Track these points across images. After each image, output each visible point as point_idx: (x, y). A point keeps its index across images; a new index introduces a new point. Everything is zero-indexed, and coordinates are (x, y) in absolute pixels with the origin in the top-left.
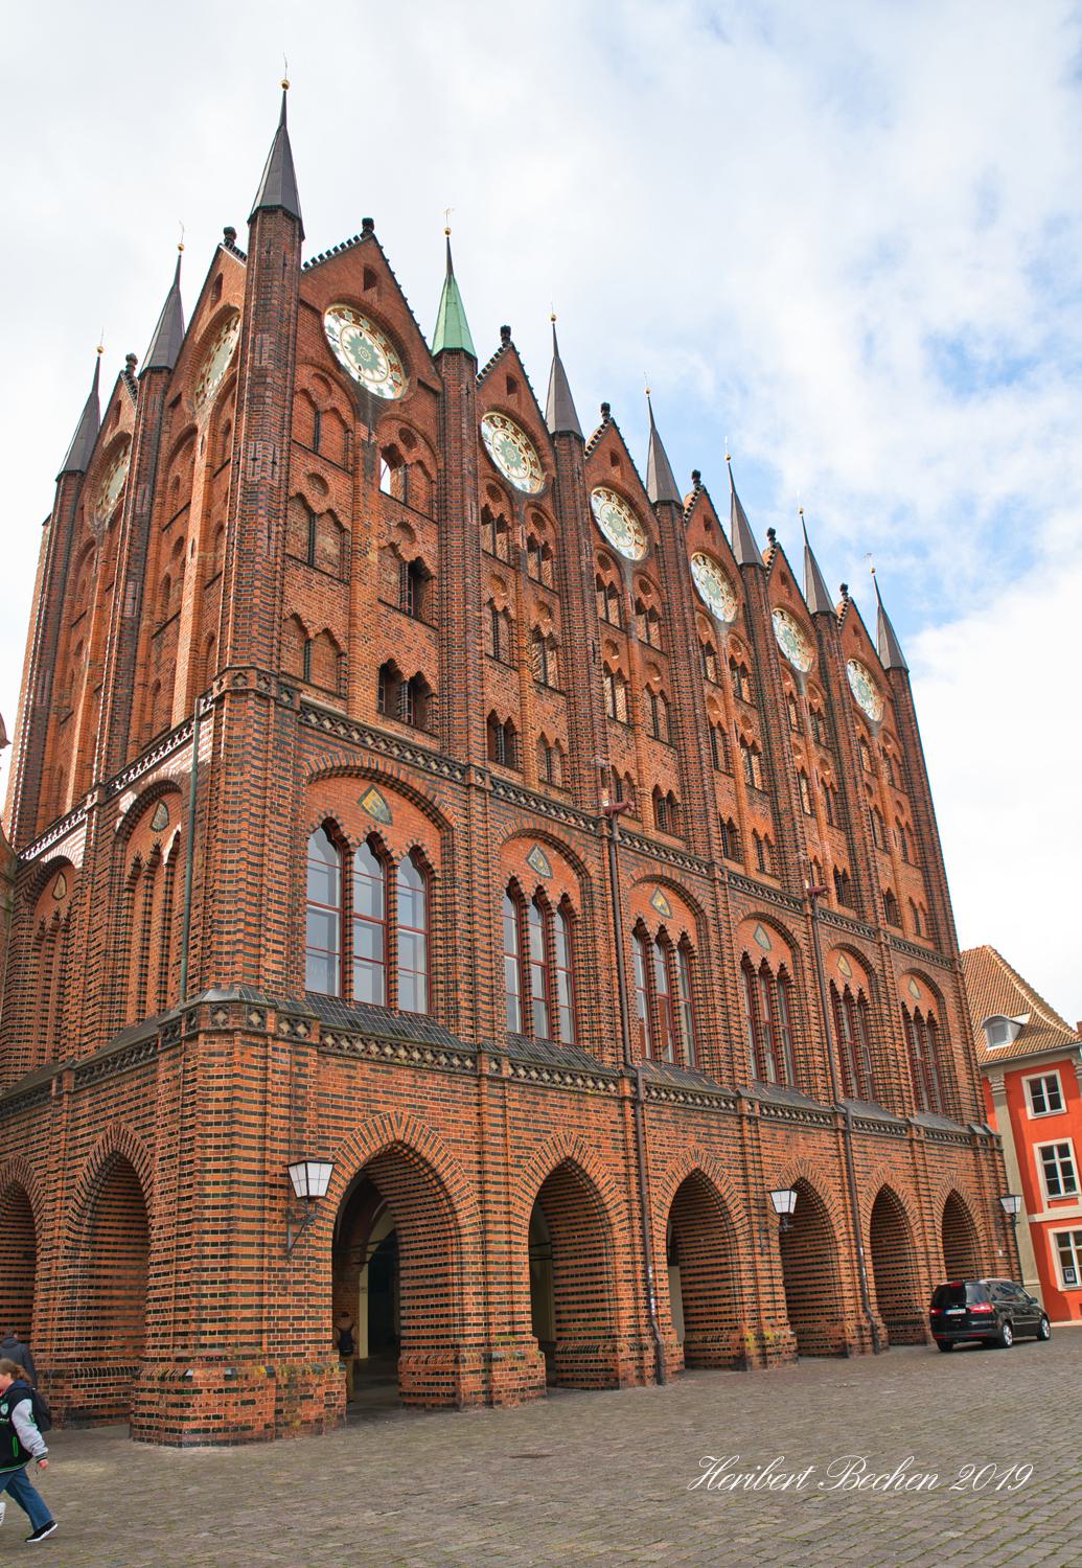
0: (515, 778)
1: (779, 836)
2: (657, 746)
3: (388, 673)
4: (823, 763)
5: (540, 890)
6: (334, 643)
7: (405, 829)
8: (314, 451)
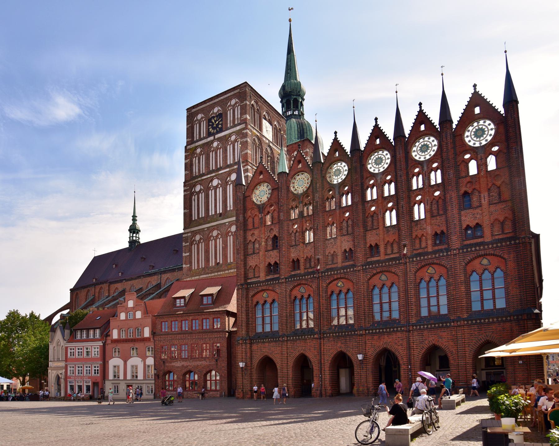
0: (298, 272)
2: (345, 238)
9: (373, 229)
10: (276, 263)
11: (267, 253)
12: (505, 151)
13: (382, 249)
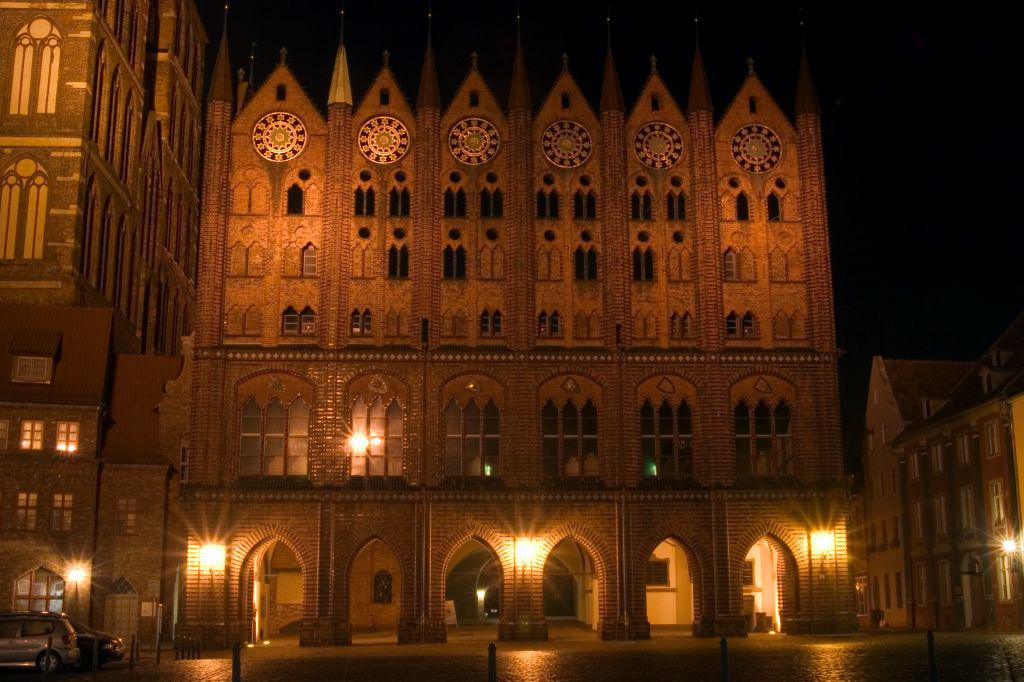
2: (489, 285)
9: (548, 280)
11: (283, 282)
12: (798, 194)
13: (568, 324)
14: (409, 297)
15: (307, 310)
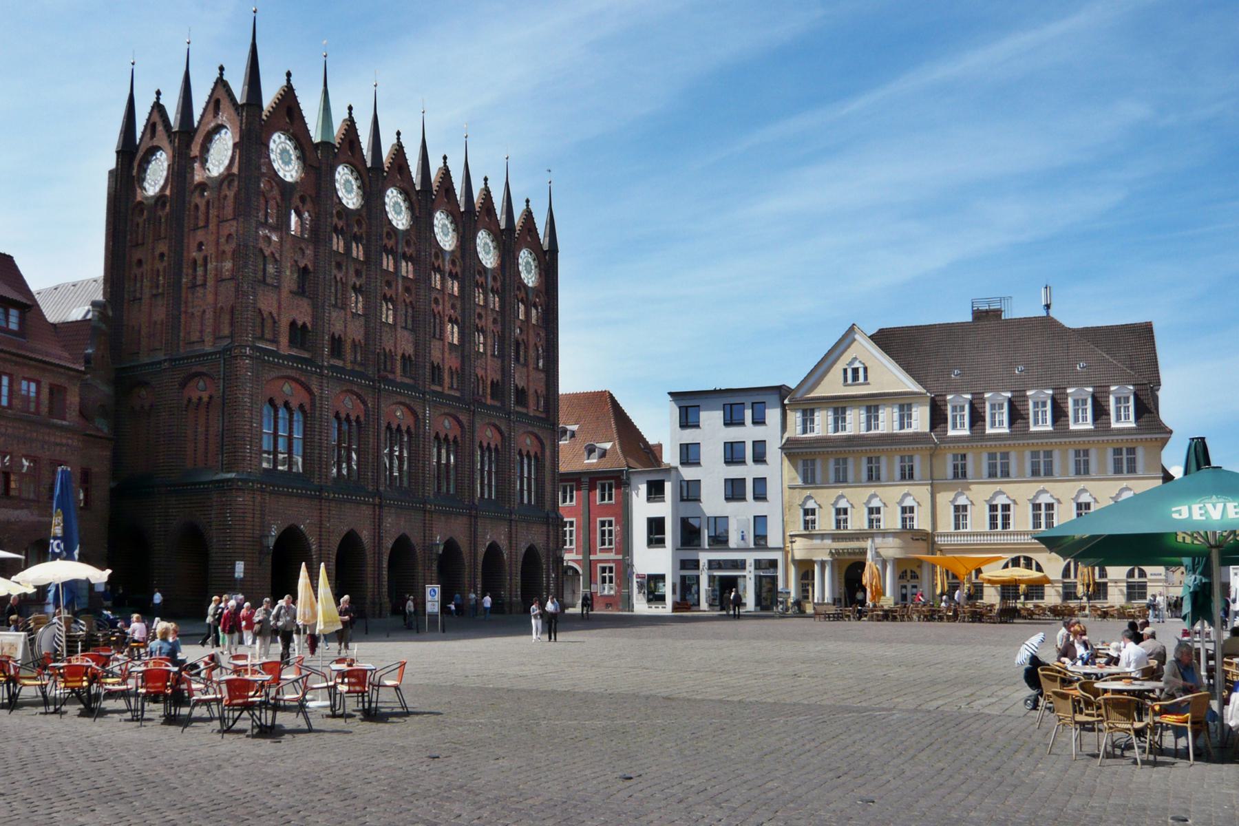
0: (340, 363)
1: (463, 369)
2: (406, 333)
3: (293, 324)
4: (495, 321)
5: (348, 416)
6: (273, 318)
7: (297, 396)
8: (265, 224)
10: (304, 325)
14: (362, 331)
15: (304, 325)
